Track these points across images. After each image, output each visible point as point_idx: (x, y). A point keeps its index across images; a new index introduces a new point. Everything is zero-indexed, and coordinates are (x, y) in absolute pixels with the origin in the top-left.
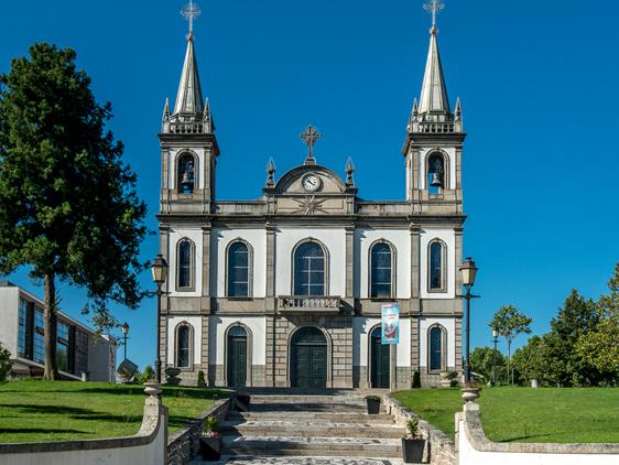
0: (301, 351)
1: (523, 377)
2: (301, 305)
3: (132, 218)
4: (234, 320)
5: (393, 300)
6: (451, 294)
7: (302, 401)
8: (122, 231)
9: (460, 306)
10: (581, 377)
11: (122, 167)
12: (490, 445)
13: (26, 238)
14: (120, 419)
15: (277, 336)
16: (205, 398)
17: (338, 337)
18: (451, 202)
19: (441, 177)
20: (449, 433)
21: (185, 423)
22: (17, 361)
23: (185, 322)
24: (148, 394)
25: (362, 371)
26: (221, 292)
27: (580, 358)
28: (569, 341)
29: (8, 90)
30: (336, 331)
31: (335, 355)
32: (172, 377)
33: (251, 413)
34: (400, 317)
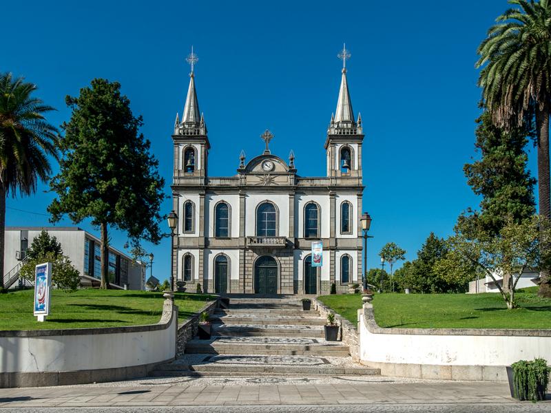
0: (261, 271)
1: (400, 287)
2: (261, 242)
4: (219, 251)
5: (319, 239)
6: (355, 235)
7: (262, 302)
8: (149, 196)
9: (361, 243)
10: (437, 287)
11: (149, 156)
12: (379, 329)
13: (89, 200)
14: (149, 313)
15: (246, 262)
17: (284, 262)
18: (355, 178)
19: (349, 162)
20: (354, 322)
21: (190, 316)
22: (84, 277)
23: (189, 253)
24: (166, 298)
25: (299, 284)
26: (211, 234)
27: (435, 276)
28: (429, 265)
30: (283, 258)
31: (283, 273)
33: (230, 310)
34: (324, 250)
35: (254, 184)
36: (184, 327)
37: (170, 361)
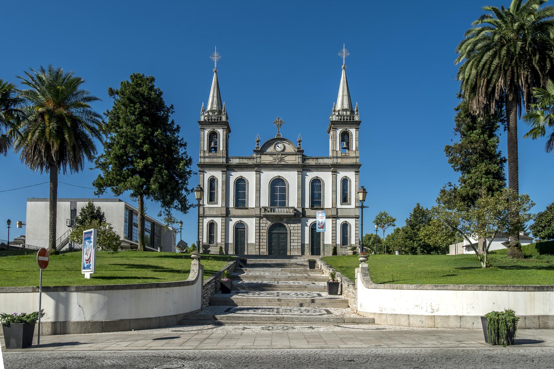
0: (274, 236)
1: (391, 249)
2: (274, 212)
5: (323, 209)
6: (353, 205)
7: (274, 262)
8: (179, 173)
9: (358, 212)
10: (422, 249)
11: (179, 139)
12: (374, 285)
14: (178, 272)
15: (261, 228)
16: (223, 260)
17: (293, 228)
18: (353, 157)
19: (348, 144)
20: (352, 279)
21: (214, 274)
22: (124, 241)
23: (213, 221)
24: (193, 258)
25: (306, 246)
26: (231, 204)
27: (421, 240)
28: (416, 231)
30: (292, 225)
31: (292, 238)
33: (248, 269)
34: (326, 218)
35: (267, 162)
36: (209, 283)
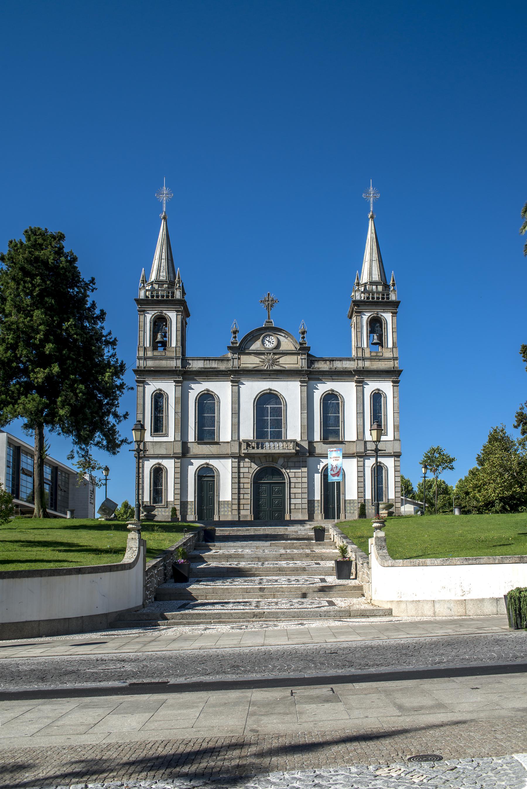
0: (264, 487)
2: (262, 448)
3: (112, 376)
4: (203, 462)
8: (103, 387)
11: (105, 333)
13: (20, 394)
15: (242, 476)
16: (177, 531)
18: (389, 359)
19: (380, 337)
23: (159, 464)
26: (191, 437)
29: (5, 267)
31: (293, 491)
32: (148, 513)
35: (251, 366)
36: (154, 567)
37: (136, 609)
